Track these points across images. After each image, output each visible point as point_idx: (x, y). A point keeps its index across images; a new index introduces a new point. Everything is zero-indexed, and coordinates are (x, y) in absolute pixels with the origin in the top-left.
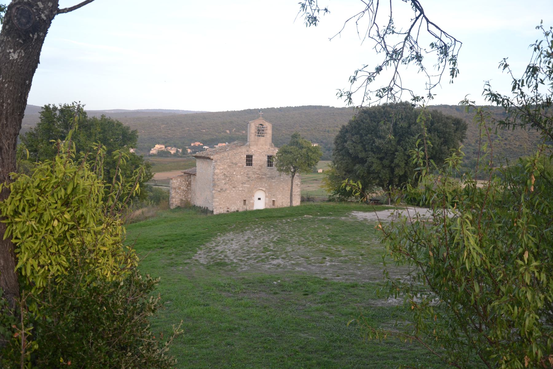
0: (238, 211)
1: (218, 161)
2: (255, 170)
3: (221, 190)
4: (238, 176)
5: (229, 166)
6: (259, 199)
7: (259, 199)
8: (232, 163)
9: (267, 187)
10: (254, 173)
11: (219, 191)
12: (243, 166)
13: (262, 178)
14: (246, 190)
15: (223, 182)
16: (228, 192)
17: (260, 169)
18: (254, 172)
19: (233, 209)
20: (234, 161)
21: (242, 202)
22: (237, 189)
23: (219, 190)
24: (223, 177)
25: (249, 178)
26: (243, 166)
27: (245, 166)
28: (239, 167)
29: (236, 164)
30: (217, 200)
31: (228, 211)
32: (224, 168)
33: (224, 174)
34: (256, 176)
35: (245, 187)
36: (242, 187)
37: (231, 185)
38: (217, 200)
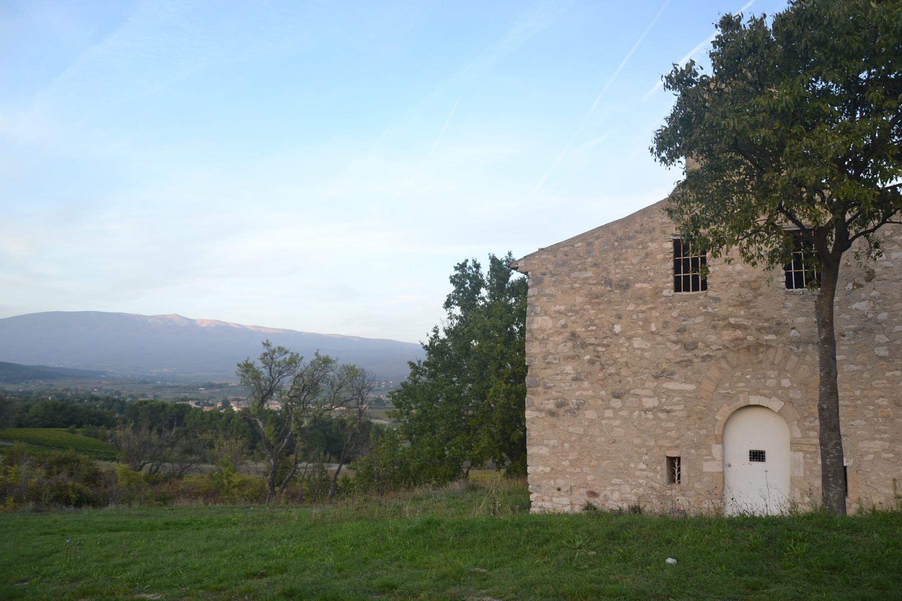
0: (636, 510)
1: (547, 279)
2: (720, 309)
3: (560, 405)
4: (637, 343)
5: (594, 297)
6: (757, 456)
7: (757, 456)
8: (608, 283)
9: (796, 395)
10: (716, 322)
11: (552, 414)
12: (657, 292)
13: (758, 347)
14: (679, 410)
15: (569, 368)
16: (591, 414)
17: (744, 303)
18: (713, 316)
19: (616, 497)
20: (616, 274)
21: (662, 468)
22: (631, 401)
23: (551, 405)
24: (566, 349)
25: (690, 347)
26: (657, 292)
27: (669, 291)
28: (640, 298)
29: (624, 286)
30: (544, 451)
31: (589, 507)
32: (572, 310)
33: (574, 335)
34: (728, 335)
35: (669, 393)
36: (656, 393)
37: (603, 383)
38: (544, 451)
